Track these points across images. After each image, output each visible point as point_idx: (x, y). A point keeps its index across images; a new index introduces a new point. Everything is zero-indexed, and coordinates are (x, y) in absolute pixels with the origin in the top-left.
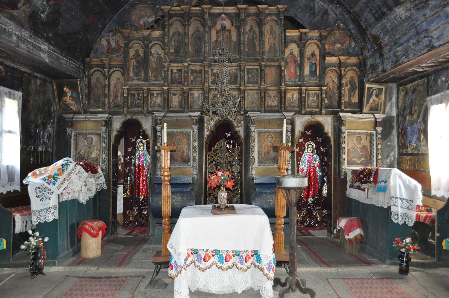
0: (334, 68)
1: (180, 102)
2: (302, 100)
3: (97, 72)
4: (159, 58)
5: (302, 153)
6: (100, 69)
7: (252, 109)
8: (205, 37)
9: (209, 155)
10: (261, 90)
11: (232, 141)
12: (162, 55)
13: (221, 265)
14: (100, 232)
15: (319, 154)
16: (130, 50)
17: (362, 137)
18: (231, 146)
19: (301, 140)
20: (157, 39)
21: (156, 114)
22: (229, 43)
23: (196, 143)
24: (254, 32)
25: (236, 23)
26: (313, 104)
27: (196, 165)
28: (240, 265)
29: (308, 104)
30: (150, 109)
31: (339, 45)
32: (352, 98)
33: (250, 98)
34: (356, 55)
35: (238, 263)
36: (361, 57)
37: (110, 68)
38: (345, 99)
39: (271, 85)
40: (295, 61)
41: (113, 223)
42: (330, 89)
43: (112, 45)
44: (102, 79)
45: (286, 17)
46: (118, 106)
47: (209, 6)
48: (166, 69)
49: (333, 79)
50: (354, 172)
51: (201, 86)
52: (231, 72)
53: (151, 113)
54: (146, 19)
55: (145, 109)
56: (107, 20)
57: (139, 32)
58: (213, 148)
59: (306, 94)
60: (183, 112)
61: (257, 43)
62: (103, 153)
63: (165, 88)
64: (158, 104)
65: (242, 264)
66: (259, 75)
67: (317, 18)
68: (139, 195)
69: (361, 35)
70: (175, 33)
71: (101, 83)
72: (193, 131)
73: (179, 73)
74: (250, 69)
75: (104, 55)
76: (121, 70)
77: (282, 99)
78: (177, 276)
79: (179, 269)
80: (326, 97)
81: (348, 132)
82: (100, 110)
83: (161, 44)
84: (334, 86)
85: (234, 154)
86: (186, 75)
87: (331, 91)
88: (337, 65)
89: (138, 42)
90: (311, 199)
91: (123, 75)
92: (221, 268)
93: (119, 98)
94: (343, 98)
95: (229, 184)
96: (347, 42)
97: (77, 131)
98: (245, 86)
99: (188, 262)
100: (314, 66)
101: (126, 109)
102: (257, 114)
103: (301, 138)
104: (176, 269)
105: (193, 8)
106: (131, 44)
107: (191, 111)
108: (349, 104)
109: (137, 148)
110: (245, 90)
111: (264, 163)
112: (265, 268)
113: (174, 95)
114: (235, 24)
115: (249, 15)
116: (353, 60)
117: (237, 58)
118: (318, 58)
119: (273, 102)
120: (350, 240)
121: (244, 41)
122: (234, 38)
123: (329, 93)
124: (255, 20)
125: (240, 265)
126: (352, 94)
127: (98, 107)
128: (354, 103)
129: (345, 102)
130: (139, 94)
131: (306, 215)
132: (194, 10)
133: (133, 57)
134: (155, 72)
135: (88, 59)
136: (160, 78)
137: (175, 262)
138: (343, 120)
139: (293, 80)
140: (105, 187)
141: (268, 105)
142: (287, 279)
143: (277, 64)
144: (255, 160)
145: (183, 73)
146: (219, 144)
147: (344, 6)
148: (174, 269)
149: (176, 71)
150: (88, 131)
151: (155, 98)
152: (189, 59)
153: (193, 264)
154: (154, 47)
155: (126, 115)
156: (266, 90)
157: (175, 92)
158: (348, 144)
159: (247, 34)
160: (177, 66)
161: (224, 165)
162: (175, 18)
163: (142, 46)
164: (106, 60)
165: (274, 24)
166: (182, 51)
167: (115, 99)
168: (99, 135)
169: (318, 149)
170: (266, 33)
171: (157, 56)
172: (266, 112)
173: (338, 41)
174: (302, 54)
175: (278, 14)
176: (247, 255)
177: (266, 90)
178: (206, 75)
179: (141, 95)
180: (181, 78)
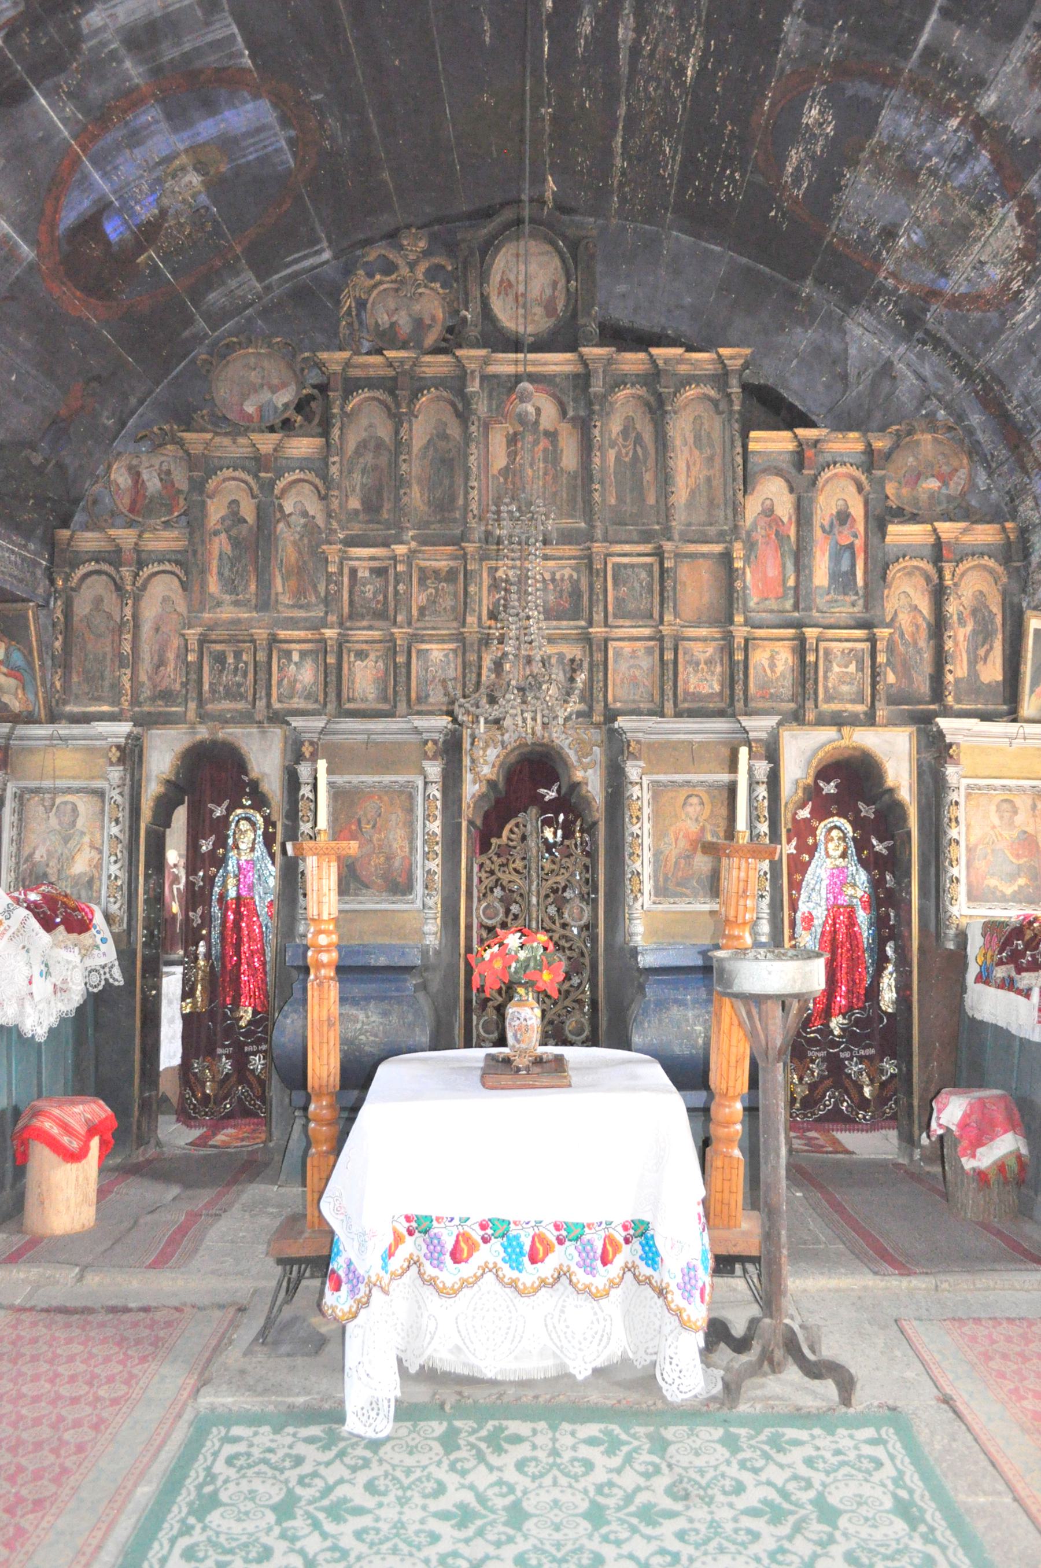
1: (382, 684)
2: (805, 675)
3: (95, 577)
4: (311, 528)
5: (806, 857)
6: (105, 567)
7: (634, 706)
8: (466, 456)
9: (481, 866)
10: (661, 639)
11: (561, 817)
13: (515, 1274)
14: (95, 1143)
15: (871, 862)
16: (209, 501)
17: (1018, 801)
18: (560, 832)
19: (805, 813)
20: (304, 464)
21: (296, 722)
22: (549, 478)
23: (438, 823)
24: (638, 440)
25: (575, 409)
26: (845, 688)
27: (435, 901)
28: (581, 1277)
29: (826, 689)
30: (277, 706)
31: (933, 484)
32: (980, 666)
33: (623, 666)
34: (995, 516)
35: (574, 1268)
36: (1009, 525)
37: (141, 564)
38: (957, 670)
39: (698, 624)
41: (145, 1106)
42: (902, 635)
43: (149, 484)
44: (111, 602)
45: (746, 387)
46: (166, 696)
47: (483, 352)
48: (332, 569)
49: (915, 602)
50: (991, 928)
51: (455, 624)
52: (558, 577)
53: (277, 718)
54: (265, 396)
55: (261, 704)
56: (133, 401)
57: (242, 440)
58: (494, 841)
60: (390, 714)
61: (648, 477)
62: (113, 858)
63: (330, 633)
64: (305, 688)
65: (591, 1271)
66: (656, 587)
67: (858, 389)
68: (236, 1004)
69: (1014, 448)
70: (363, 445)
71: (109, 616)
72: (426, 783)
73: (379, 582)
74: (625, 566)
75: (119, 521)
76: (177, 570)
77: (735, 672)
78: (355, 1317)
79: (363, 1288)
80: (889, 663)
81: (968, 787)
82: (105, 708)
83: (317, 481)
84: (917, 627)
85: (568, 862)
86: (401, 587)
87: (906, 644)
88: (927, 552)
89: (237, 474)
90: (840, 1019)
91: (185, 589)
92: (513, 1284)
93: (170, 668)
94: (948, 667)
95: (546, 976)
96: (963, 473)
97: (23, 784)
98: (606, 625)
99: (397, 1263)
100: (847, 555)
101: (192, 705)
102: (651, 722)
103: (803, 806)
104: (353, 1290)
105: (428, 358)
106: (211, 484)
107: (419, 713)
108: (973, 687)
109: (230, 841)
110: (606, 641)
111: (675, 895)
112: (673, 1287)
113: (361, 655)
114: (571, 413)
115: (619, 382)
116: (985, 534)
117: (577, 530)
118: (860, 527)
119: (703, 681)
120: (981, 1176)
121: (603, 469)
122: (570, 460)
123: (902, 649)
124: (640, 397)
125: (581, 1277)
126: (982, 652)
127: (98, 700)
128: (989, 685)
129: (957, 681)
130: (238, 655)
131: (822, 1078)
132: (429, 365)
133: (219, 527)
135: (66, 533)
137: (350, 1263)
138: (950, 745)
139: (772, 604)
140: (118, 978)
141: (686, 693)
142: (753, 1323)
143: (718, 548)
144: (641, 882)
145: (391, 579)
146: (517, 825)
147: (947, 349)
148: (344, 1288)
149: (367, 574)
150: (61, 783)
151: (292, 667)
152: (411, 534)
153: (414, 1269)
154: (293, 491)
155: (193, 726)
156: (678, 639)
157: (364, 646)
158: (968, 826)
159: (613, 444)
160: (372, 558)
161: (534, 900)
162: (366, 394)
163: (251, 489)
164: (126, 536)
165: (704, 410)
166: (387, 506)
168: (100, 794)
169: (861, 844)
170: (678, 442)
171: (303, 521)
172: (678, 714)
173: (930, 467)
174: (803, 514)
175: (721, 378)
176: (609, 1240)
177: (678, 639)
178: (472, 589)
179: (245, 657)
180: (386, 597)
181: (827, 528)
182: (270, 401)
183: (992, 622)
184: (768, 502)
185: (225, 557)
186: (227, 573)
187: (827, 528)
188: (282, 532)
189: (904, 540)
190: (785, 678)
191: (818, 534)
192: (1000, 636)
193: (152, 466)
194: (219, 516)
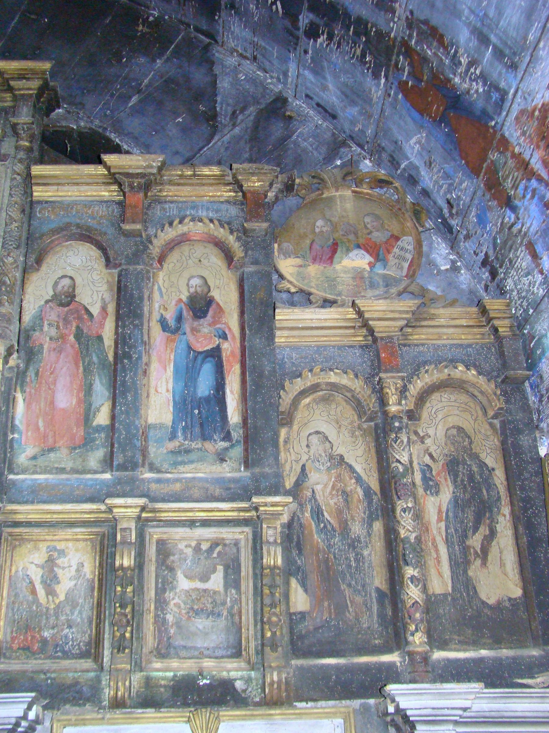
0: (333, 378)
29: (161, 623)
32: (475, 570)
40: (86, 342)
42: (318, 513)
49: (340, 450)
59: (151, 551)
84: (346, 495)
100: (207, 370)
118: (232, 322)
123: (317, 538)
126: (475, 541)
128: (498, 607)
129: (431, 604)
174: (128, 303)
181: (172, 323)
183: (490, 486)
184: (66, 282)
187: (172, 323)
189: (312, 339)
190: (74, 606)
191: (157, 335)
192: (506, 510)
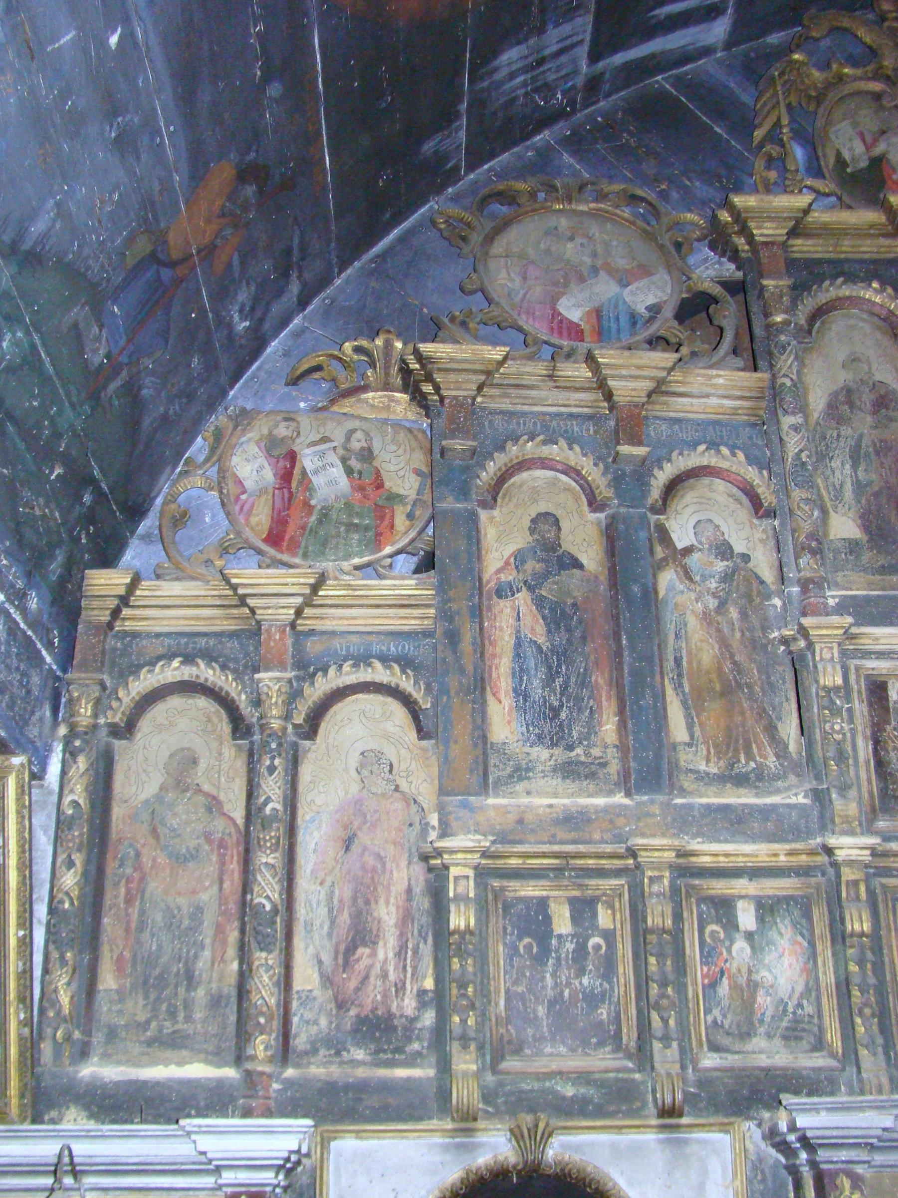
3: (175, 702)
12: (763, 564)
16: (483, 515)
37: (307, 668)
43: (318, 481)
46: (380, 1031)
55: (665, 1057)
70: (843, 403)
71: (214, 805)
82: (198, 1070)
89: (553, 451)
91: (422, 733)
93: (386, 950)
127: (172, 1043)
130: (583, 909)
134: (714, 707)
136: (771, 761)
151: (740, 946)
167: (347, 954)
171: (720, 566)
179: (604, 918)
182: (617, 301)
185: (529, 651)
186: (537, 690)
188: (671, 588)
193: (325, 440)
194: (509, 549)
